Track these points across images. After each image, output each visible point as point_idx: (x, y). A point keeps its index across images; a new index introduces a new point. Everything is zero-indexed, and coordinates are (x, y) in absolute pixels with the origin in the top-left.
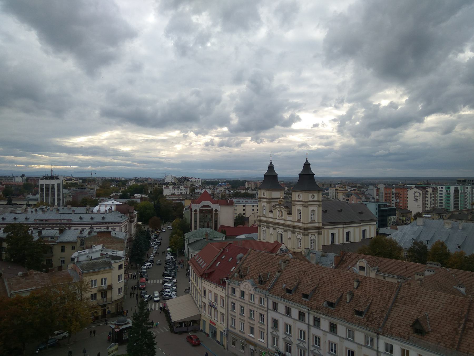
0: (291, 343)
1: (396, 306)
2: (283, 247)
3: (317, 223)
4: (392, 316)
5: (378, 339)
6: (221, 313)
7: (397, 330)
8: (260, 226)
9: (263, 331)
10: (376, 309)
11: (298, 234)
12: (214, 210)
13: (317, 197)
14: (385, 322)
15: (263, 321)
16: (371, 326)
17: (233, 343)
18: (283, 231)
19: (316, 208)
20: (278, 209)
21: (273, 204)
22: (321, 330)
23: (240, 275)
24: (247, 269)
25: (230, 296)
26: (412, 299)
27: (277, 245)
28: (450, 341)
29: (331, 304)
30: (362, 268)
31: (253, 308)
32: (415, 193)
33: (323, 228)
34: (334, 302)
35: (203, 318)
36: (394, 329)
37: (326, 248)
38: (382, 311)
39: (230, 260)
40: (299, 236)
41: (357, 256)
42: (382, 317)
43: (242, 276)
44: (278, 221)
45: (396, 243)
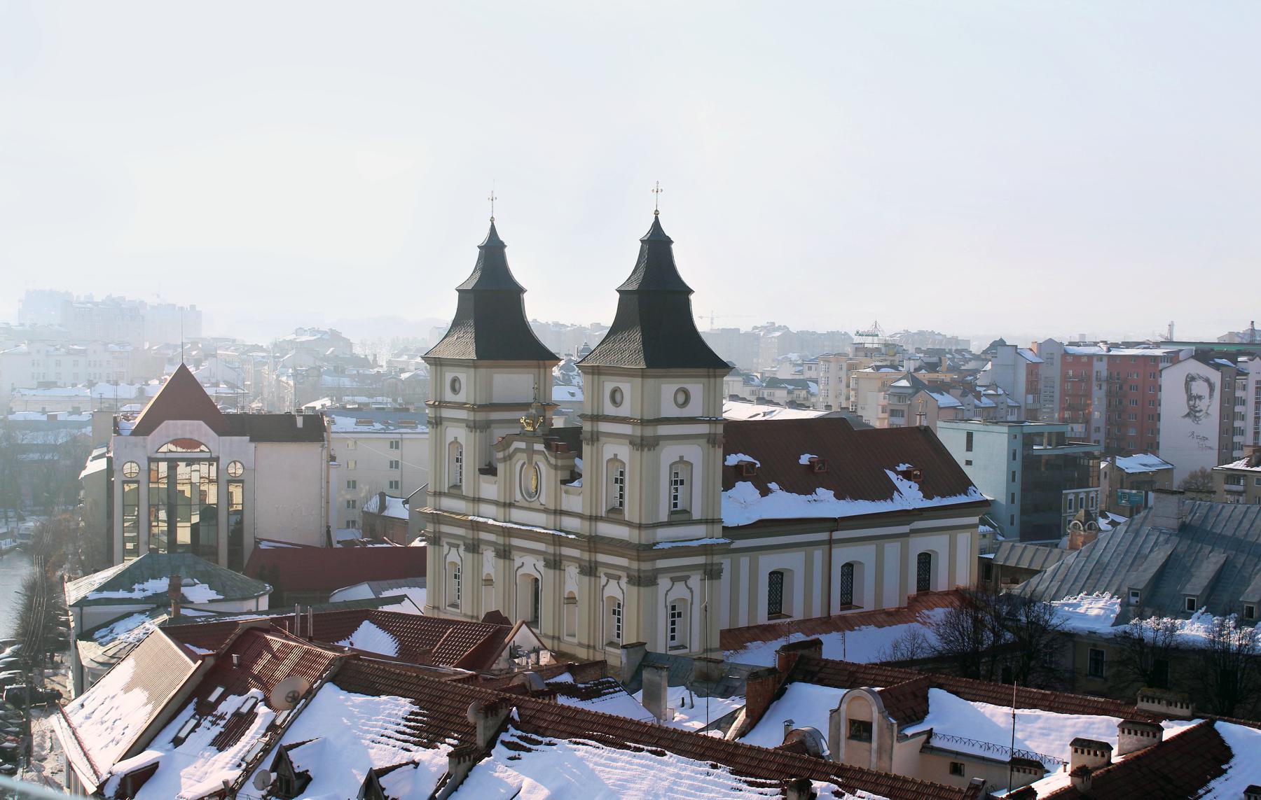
3: (699, 522)
11: (609, 576)
19: (694, 453)
20: (521, 459)
21: (498, 433)
32: (1190, 379)
40: (613, 590)
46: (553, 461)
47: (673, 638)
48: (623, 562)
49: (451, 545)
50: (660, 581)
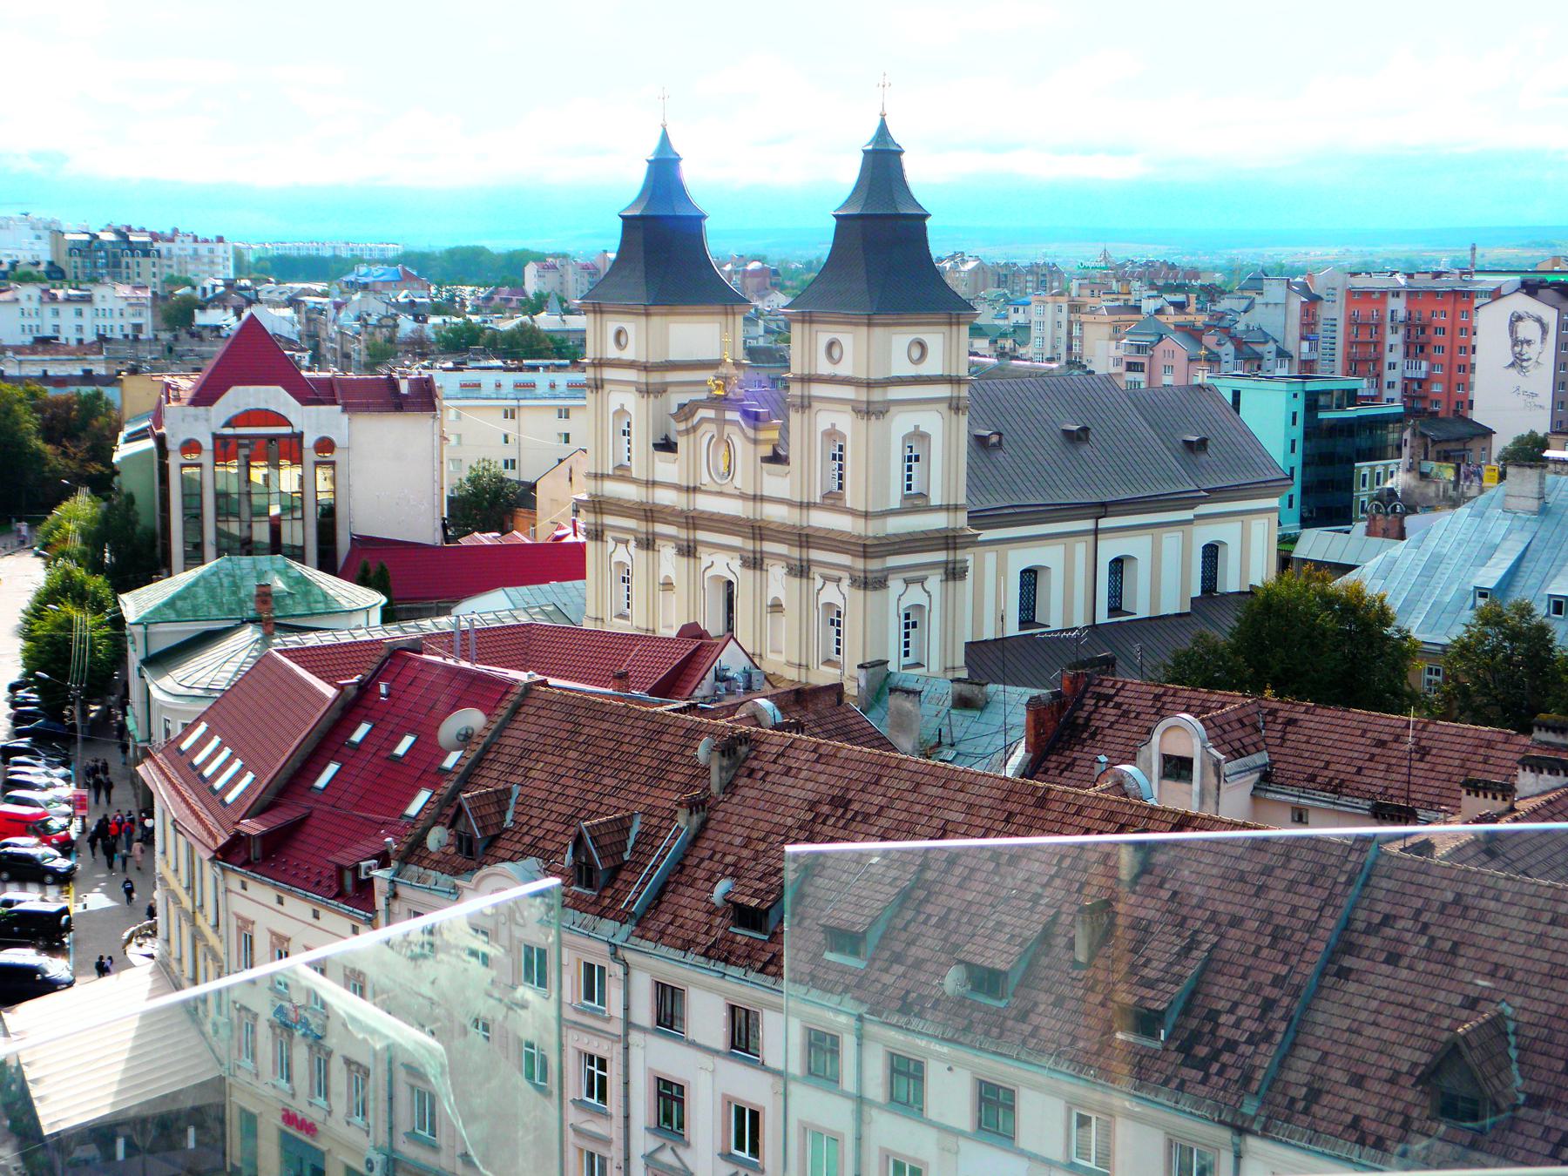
1: (1344, 974)
2: (731, 660)
3: (940, 508)
4: (1319, 1031)
5: (1238, 1157)
6: (348, 1062)
7: (1342, 1104)
8: (597, 534)
9: (599, 1150)
10: (1237, 996)
11: (826, 579)
12: (309, 441)
13: (942, 349)
14: (1282, 1064)
15: (603, 1096)
16: (1203, 1090)
18: (736, 564)
19: (932, 422)
20: (709, 430)
21: (677, 398)
23: (459, 837)
24: (501, 798)
26: (1433, 931)
27: (696, 648)
29: (986, 980)
30: (1177, 768)
32: (1517, 318)
33: (973, 542)
34: (1000, 965)
36: (1326, 1099)
37: (988, 660)
38: (1269, 1005)
40: (831, 594)
41: (1157, 697)
42: (1268, 1036)
43: (470, 840)
44: (705, 503)
45: (1384, 617)
46: (751, 433)
47: (907, 654)
48: (845, 559)
49: (617, 541)
50: (890, 583)
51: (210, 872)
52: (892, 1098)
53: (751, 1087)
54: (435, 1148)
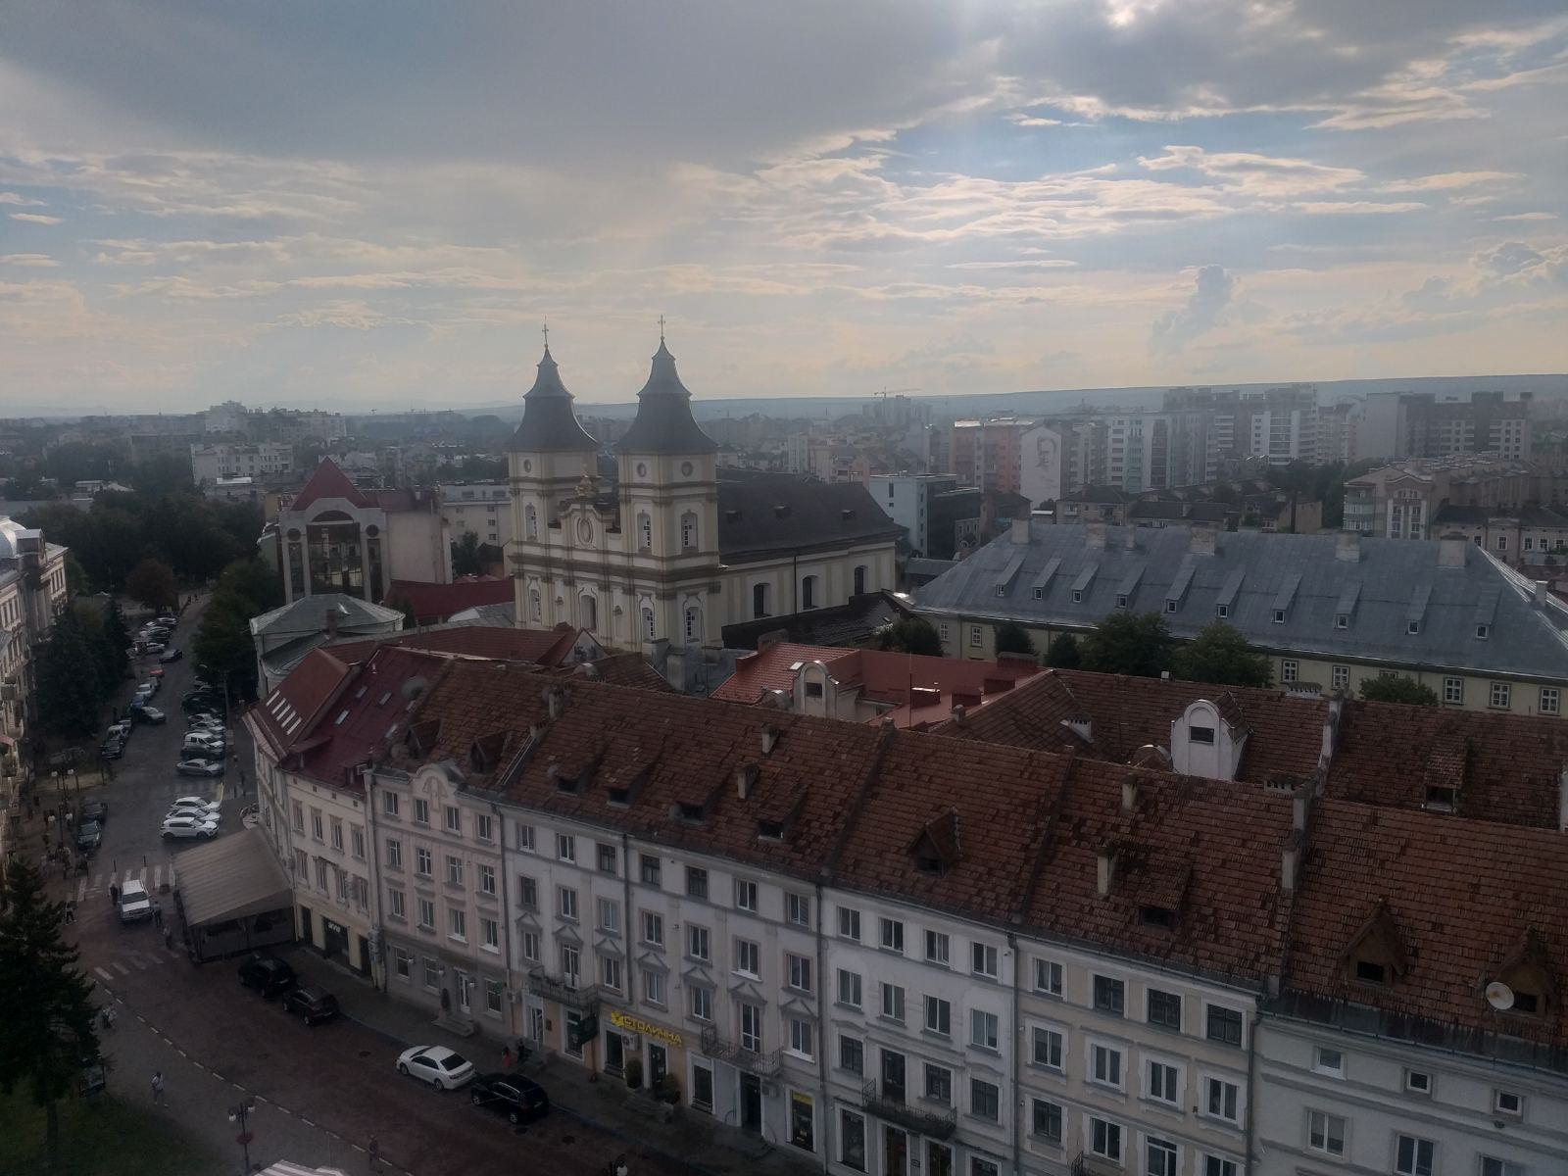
0: (578, 944)
1: (875, 796)
5: (820, 898)
8: (521, 575)
9: (493, 919)
11: (643, 595)
12: (363, 528)
15: (492, 889)
17: (404, 969)
18: (595, 589)
19: (697, 507)
20: (578, 515)
21: (561, 498)
22: (664, 893)
25: (381, 820)
28: (1008, 883)
29: (691, 811)
31: (457, 854)
32: (1040, 440)
35: (301, 901)
39: (384, 701)
40: (646, 603)
44: (578, 556)
47: (689, 634)
49: (532, 579)
50: (679, 596)
51: (278, 776)
52: (644, 879)
53: (572, 880)
54: (405, 923)
